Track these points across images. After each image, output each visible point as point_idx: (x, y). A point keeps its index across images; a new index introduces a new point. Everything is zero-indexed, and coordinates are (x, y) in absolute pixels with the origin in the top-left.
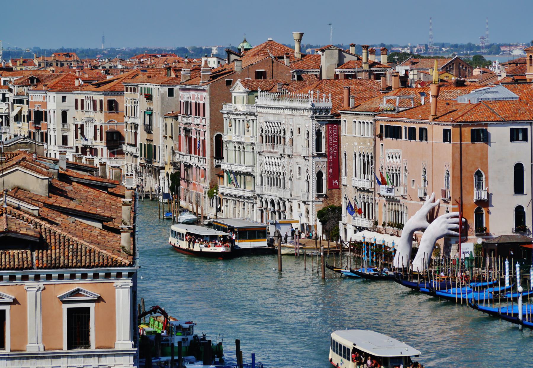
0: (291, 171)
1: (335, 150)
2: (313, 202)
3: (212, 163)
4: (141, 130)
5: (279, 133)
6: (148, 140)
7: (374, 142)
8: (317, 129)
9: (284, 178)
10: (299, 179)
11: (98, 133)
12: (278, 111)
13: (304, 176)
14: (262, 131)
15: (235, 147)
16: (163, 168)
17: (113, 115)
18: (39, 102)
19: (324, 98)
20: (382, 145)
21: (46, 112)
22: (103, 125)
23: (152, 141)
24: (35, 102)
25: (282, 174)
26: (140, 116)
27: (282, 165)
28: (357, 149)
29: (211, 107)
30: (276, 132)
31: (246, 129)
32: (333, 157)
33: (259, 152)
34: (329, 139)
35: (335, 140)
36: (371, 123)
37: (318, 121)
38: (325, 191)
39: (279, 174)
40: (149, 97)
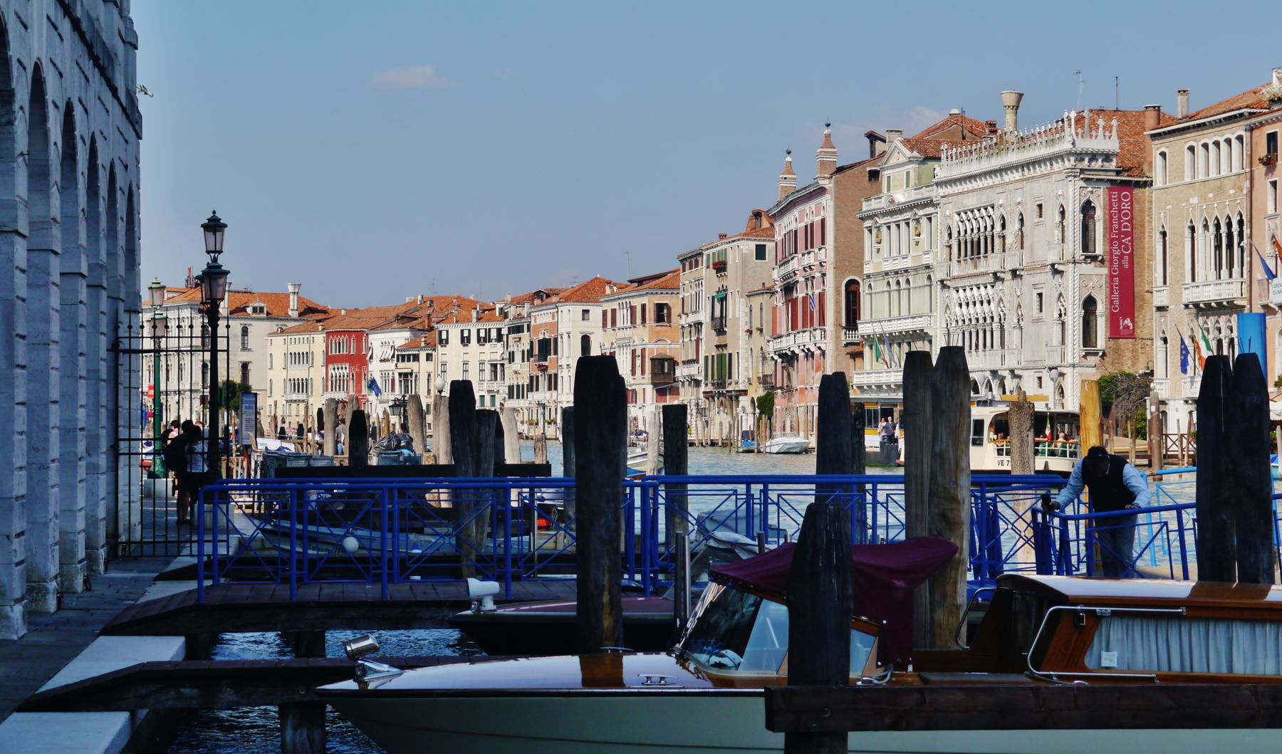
0: (1019, 306)
1: (1126, 249)
2: (1074, 366)
3: (838, 338)
4: (707, 333)
5: (989, 228)
6: (718, 347)
7: (1247, 184)
8: (1084, 200)
9: (1002, 327)
10: (1038, 320)
11: (638, 362)
12: (989, 181)
13: (1051, 310)
14: (950, 235)
15: (889, 284)
16: (745, 392)
17: (662, 329)
18: (546, 324)
19: (1101, 130)
20: (1274, 184)
21: (556, 340)
22: (647, 347)
23: (726, 346)
24: (541, 325)
25: (996, 319)
26: (706, 306)
27: (997, 299)
28: (1197, 214)
29: (836, 223)
30: (982, 229)
31: (913, 237)
32: (1121, 266)
33: (942, 282)
34: (1111, 224)
35: (1126, 227)
36: (1240, 138)
37: (1087, 180)
38: (1101, 341)
39: (989, 321)
40: (720, 267)
